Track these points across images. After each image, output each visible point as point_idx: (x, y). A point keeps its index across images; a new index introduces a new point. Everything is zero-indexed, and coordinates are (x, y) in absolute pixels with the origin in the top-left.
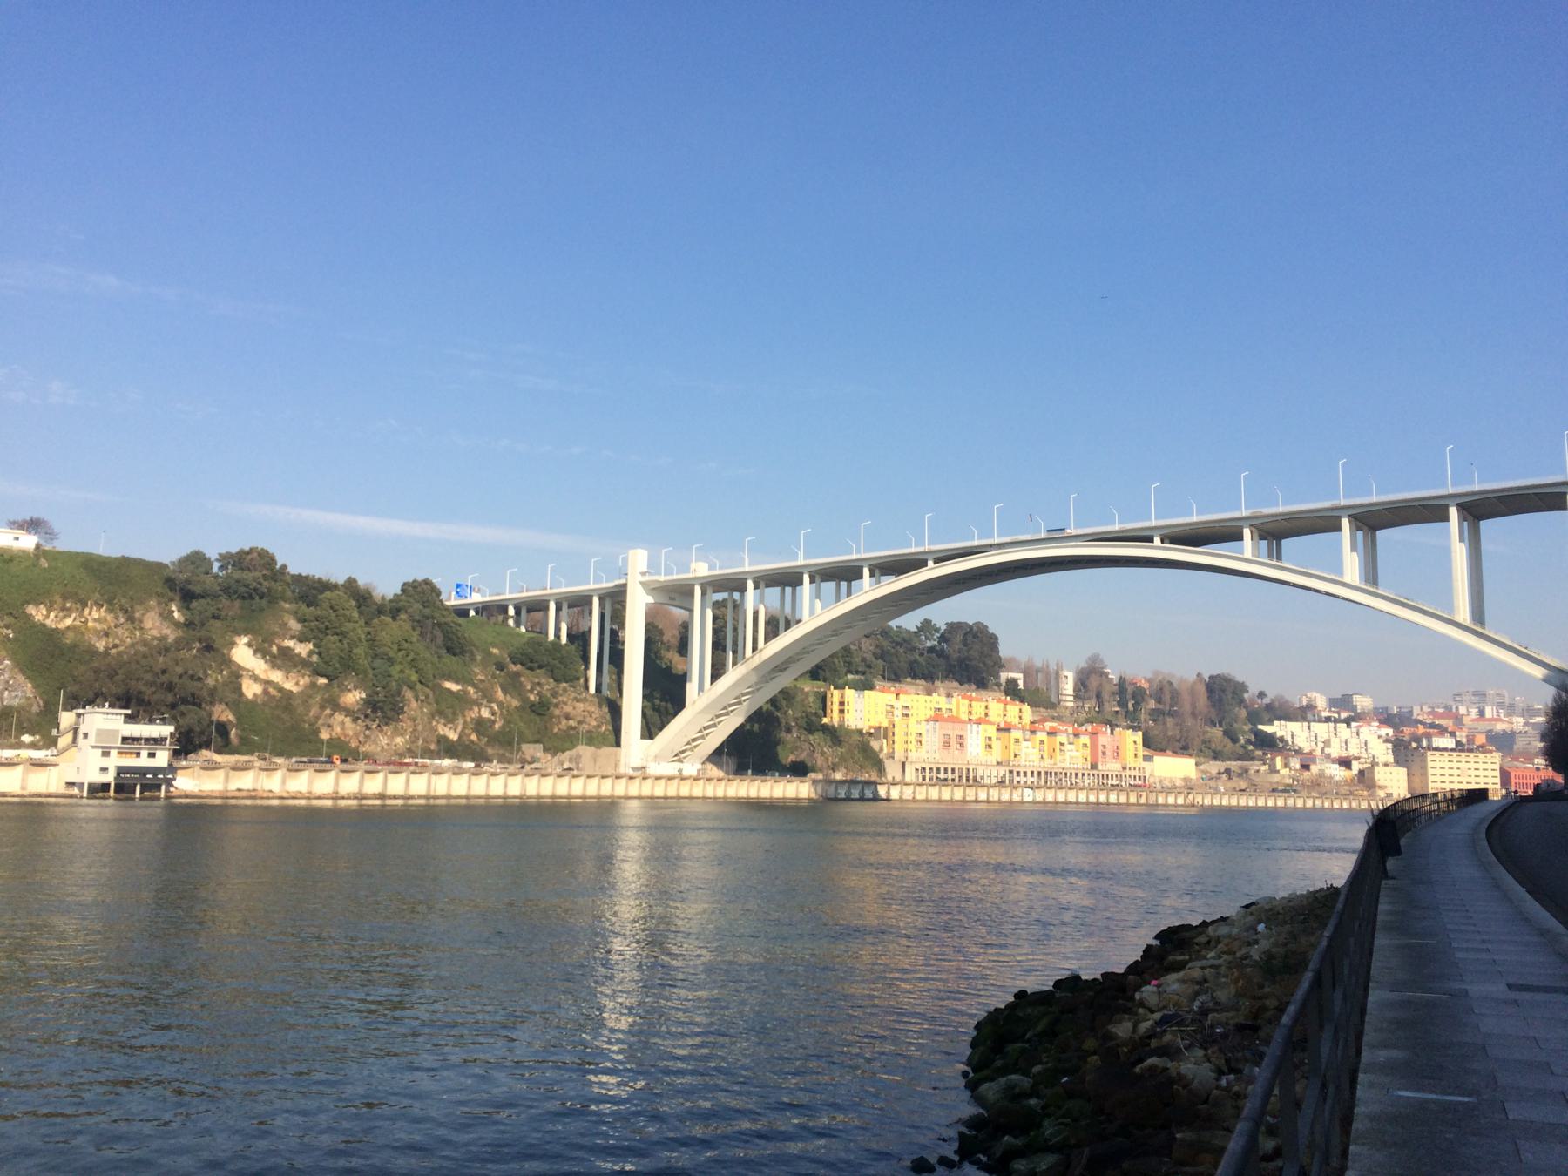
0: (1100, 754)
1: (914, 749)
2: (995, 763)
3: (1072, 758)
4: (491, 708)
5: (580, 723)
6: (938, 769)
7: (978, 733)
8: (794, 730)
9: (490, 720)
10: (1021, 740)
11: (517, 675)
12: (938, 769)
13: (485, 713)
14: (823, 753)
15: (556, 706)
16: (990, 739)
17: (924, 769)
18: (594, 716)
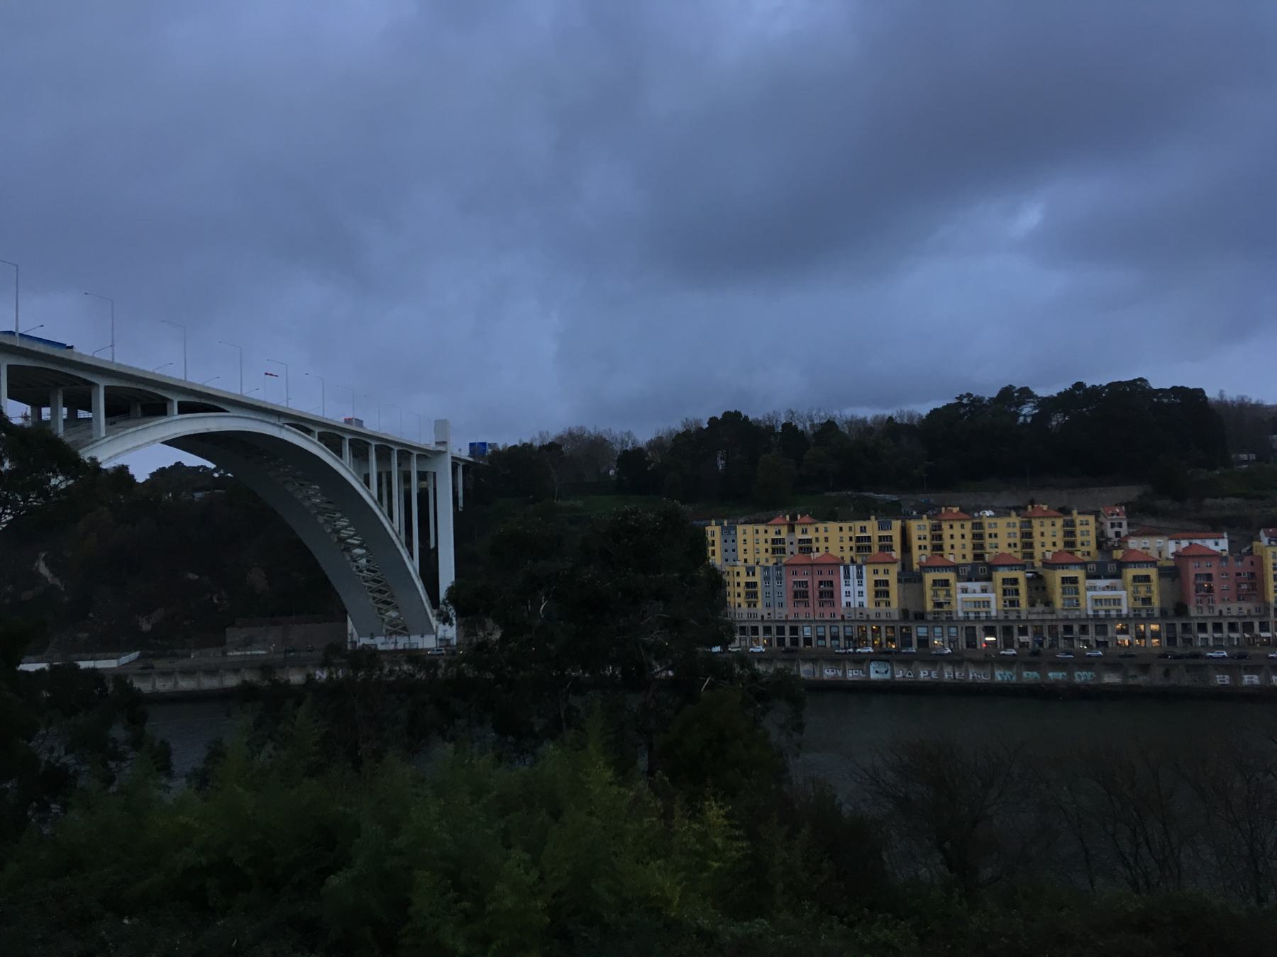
0: (1192, 588)
1: (744, 606)
2: (896, 616)
3: (1097, 601)
6: (781, 630)
7: (860, 576)
10: (952, 581)
12: (781, 630)
16: (886, 583)
17: (757, 627)
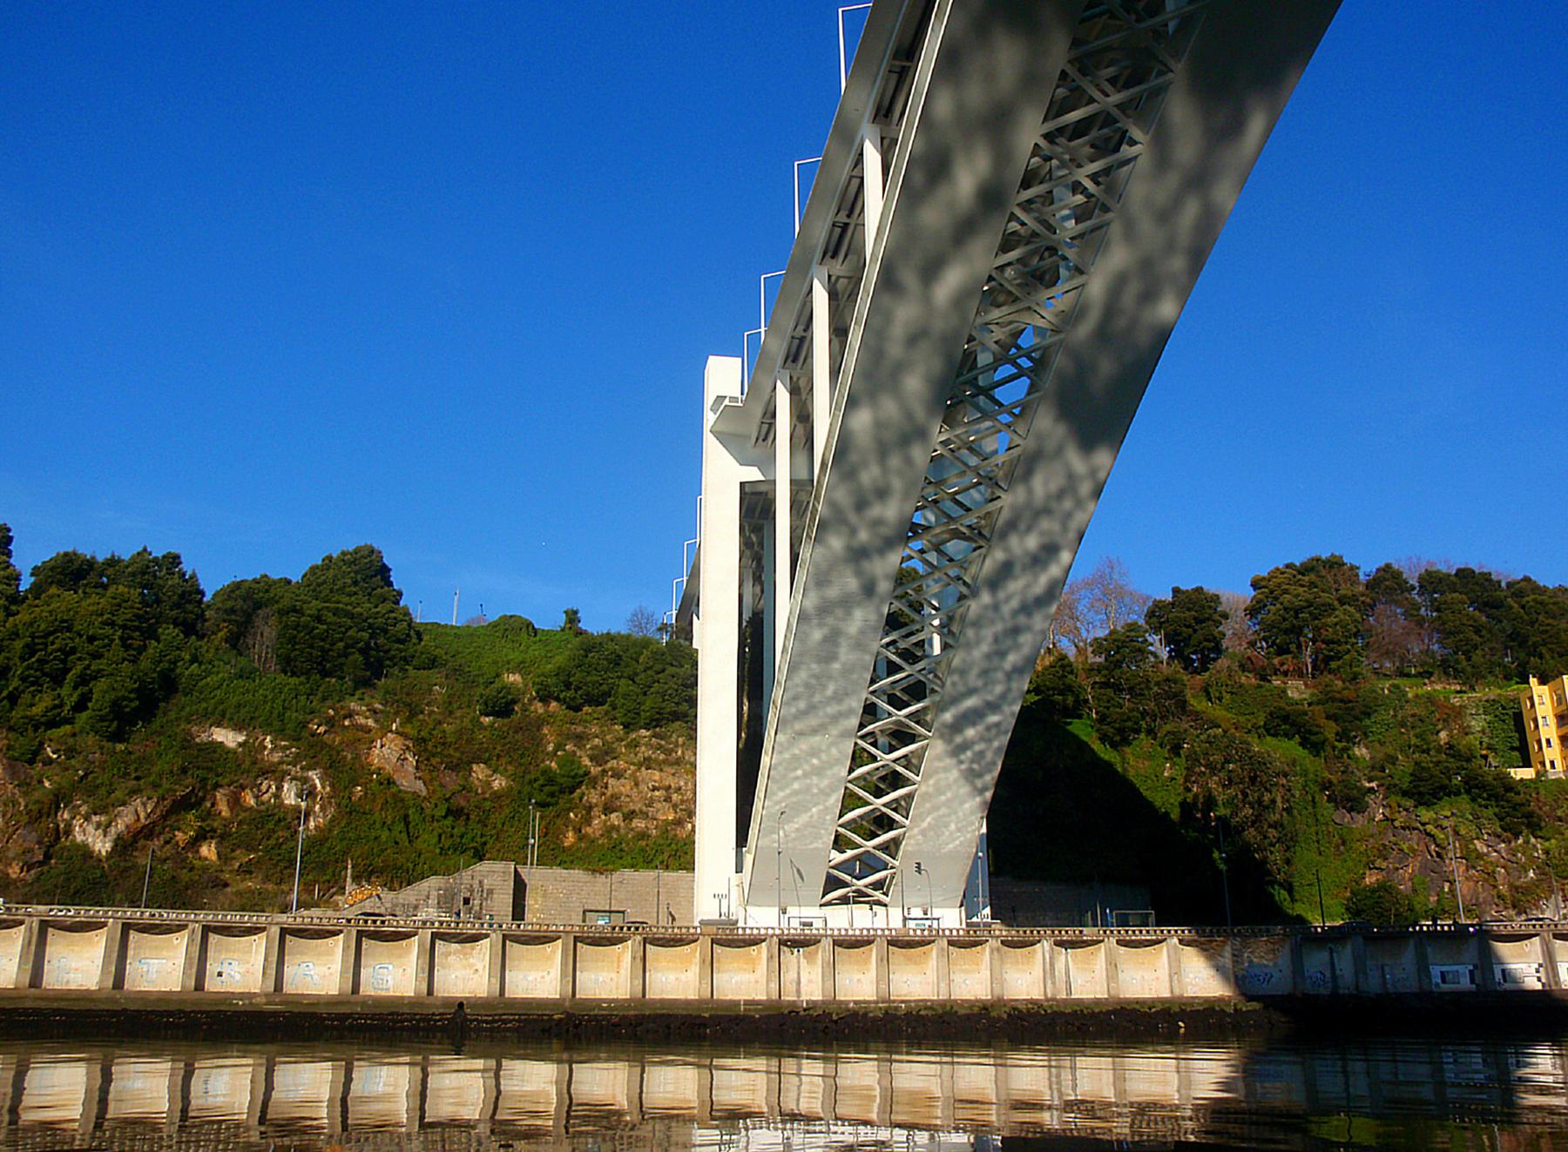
4: (305, 780)
5: (629, 816)
8: (1370, 799)
9: (297, 809)
11: (540, 722)
13: (290, 797)
14: (1471, 858)
15: (593, 782)
18: (675, 797)
